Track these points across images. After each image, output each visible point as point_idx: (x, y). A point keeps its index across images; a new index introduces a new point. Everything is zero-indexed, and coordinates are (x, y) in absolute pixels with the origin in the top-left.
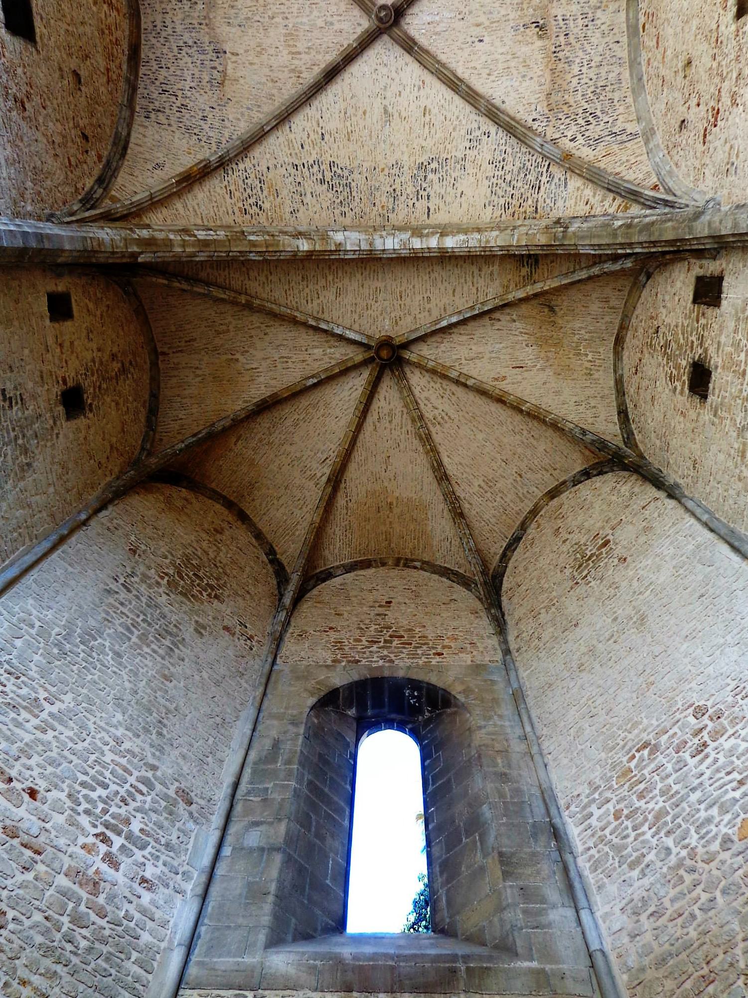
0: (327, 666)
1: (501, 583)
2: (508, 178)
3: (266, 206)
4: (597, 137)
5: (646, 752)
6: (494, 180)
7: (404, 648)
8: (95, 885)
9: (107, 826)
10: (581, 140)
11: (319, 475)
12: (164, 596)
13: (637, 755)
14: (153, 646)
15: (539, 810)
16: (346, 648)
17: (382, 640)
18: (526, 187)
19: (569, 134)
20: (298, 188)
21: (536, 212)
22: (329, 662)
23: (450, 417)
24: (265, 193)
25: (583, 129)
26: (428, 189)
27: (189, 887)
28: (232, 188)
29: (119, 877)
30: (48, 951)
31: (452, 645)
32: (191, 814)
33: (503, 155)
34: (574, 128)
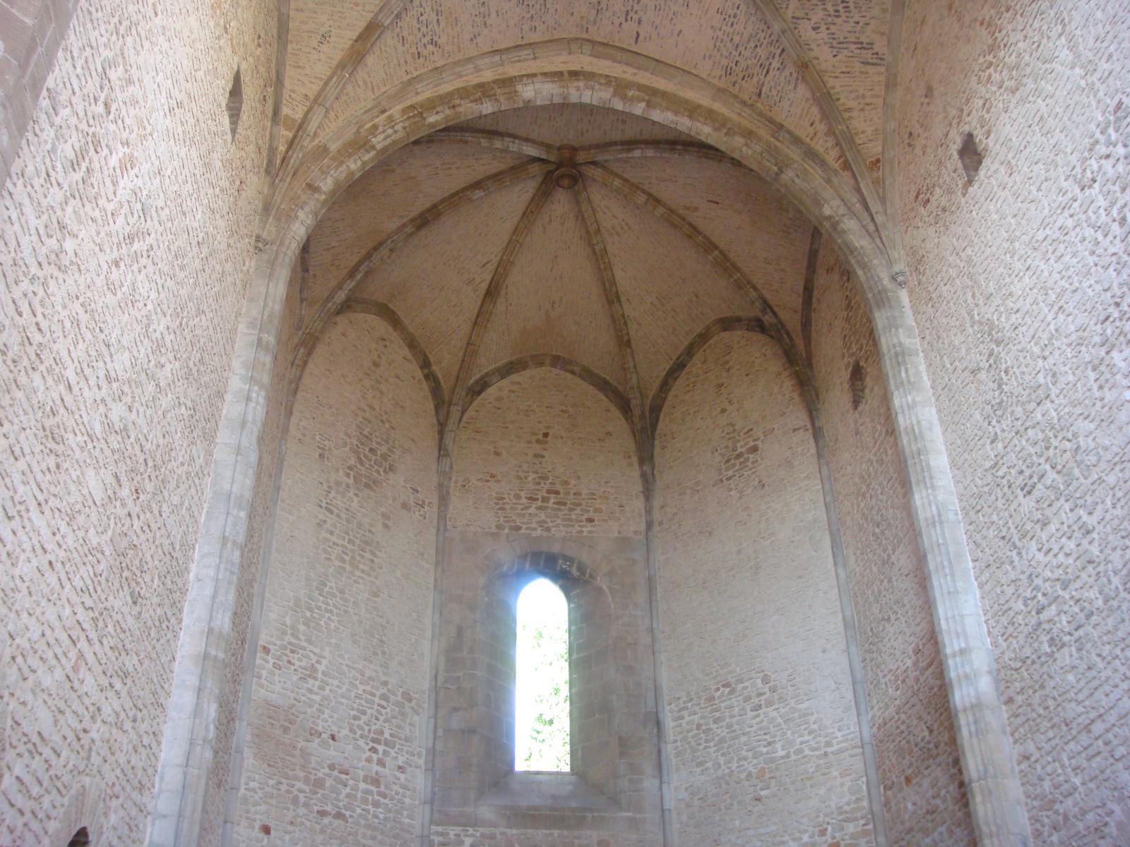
0: (493, 534)
1: (657, 421)
2: (737, 39)
3: (443, 40)
4: (842, 40)
5: (727, 690)
6: (720, 34)
7: (559, 509)
8: (376, 782)
9: (373, 741)
10: (823, 34)
11: (478, 280)
12: (356, 499)
13: (722, 689)
14: (361, 566)
15: (651, 703)
16: (507, 507)
17: (540, 497)
18: (755, 61)
19: (815, 19)
20: (482, 10)
21: (759, 95)
22: (494, 530)
23: (630, 228)
24: (443, 24)
25: (830, 20)
26: (640, 13)
27: (421, 762)
28: (405, 33)
29: (386, 771)
30: (368, 826)
31: (603, 507)
32: (413, 708)
33: (735, 11)
34: (821, 14)
